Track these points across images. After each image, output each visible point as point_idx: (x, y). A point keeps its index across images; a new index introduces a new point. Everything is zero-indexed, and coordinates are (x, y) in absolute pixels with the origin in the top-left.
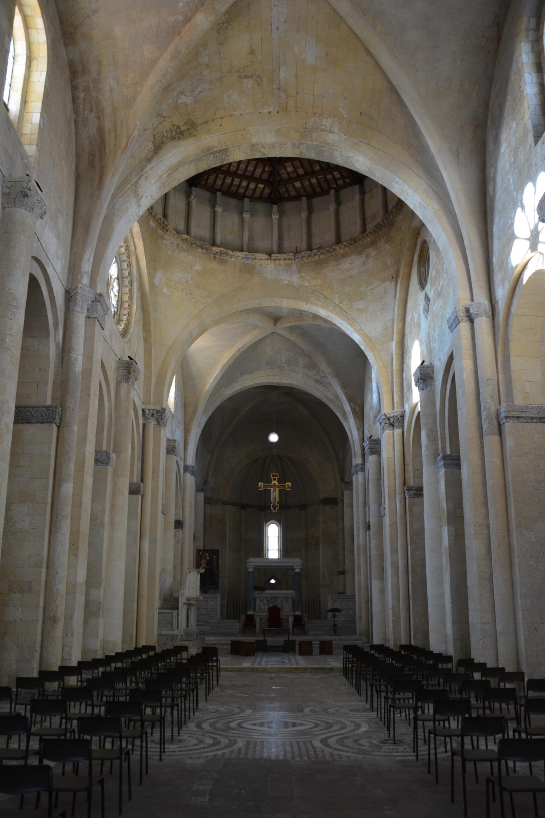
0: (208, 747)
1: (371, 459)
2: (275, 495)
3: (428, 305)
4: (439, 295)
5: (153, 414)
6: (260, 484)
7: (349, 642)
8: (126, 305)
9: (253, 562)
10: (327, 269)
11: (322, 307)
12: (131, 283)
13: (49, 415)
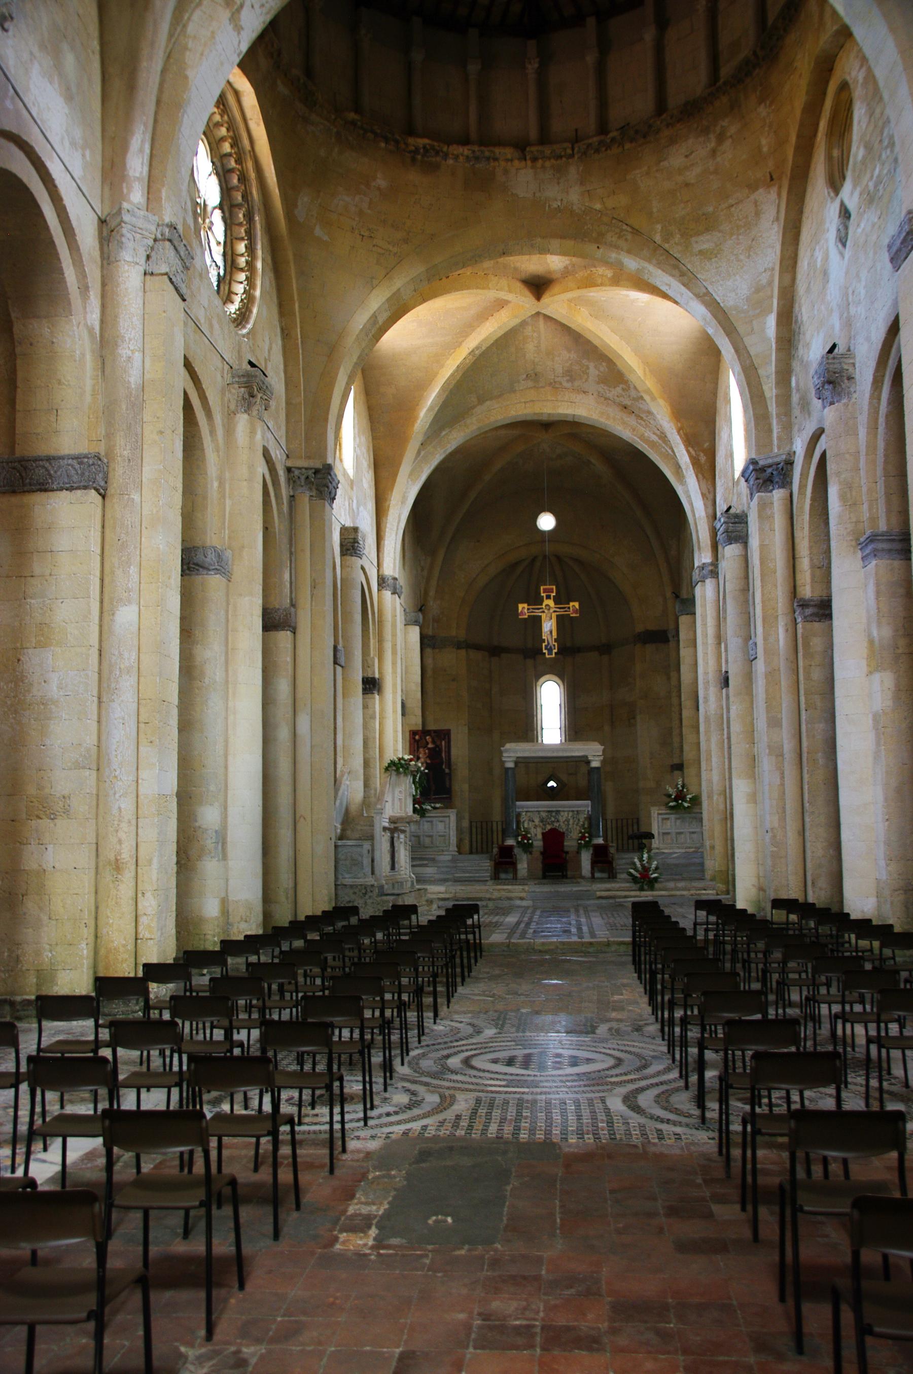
0: (396, 1113)
1: (730, 552)
2: (549, 626)
3: (846, 228)
4: (870, 199)
5: (307, 477)
6: (521, 606)
7: (692, 892)
8: (242, 262)
9: (513, 751)
10: (638, 171)
11: (629, 252)
12: (249, 217)
13: (83, 474)
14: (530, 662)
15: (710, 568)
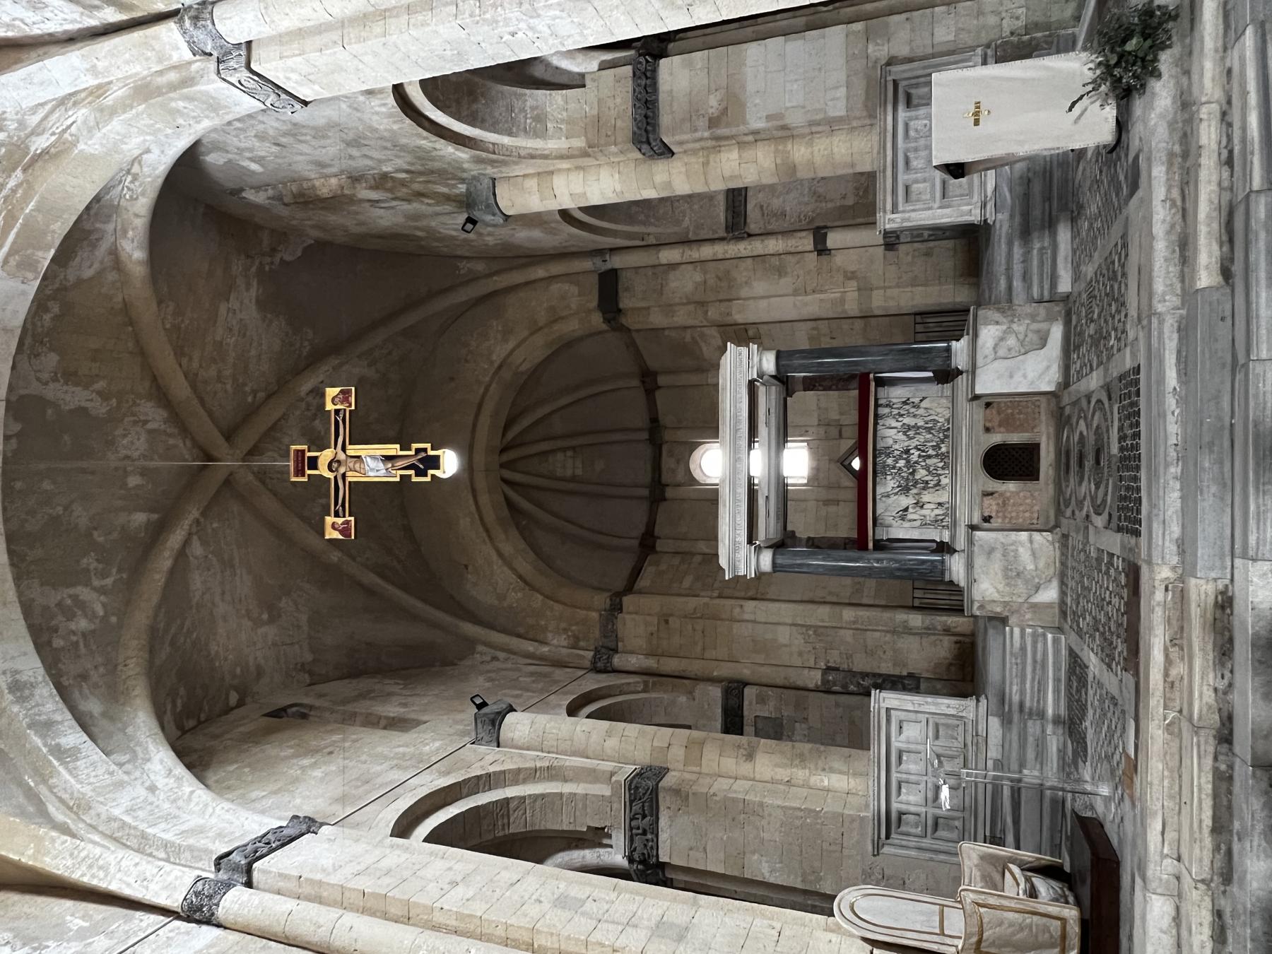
2: (373, 463)
14: (669, 493)
15: (187, 23)
